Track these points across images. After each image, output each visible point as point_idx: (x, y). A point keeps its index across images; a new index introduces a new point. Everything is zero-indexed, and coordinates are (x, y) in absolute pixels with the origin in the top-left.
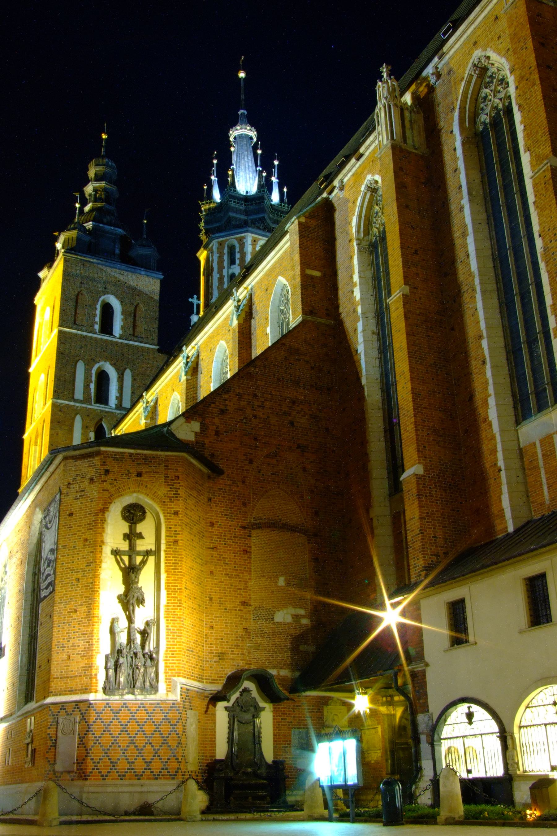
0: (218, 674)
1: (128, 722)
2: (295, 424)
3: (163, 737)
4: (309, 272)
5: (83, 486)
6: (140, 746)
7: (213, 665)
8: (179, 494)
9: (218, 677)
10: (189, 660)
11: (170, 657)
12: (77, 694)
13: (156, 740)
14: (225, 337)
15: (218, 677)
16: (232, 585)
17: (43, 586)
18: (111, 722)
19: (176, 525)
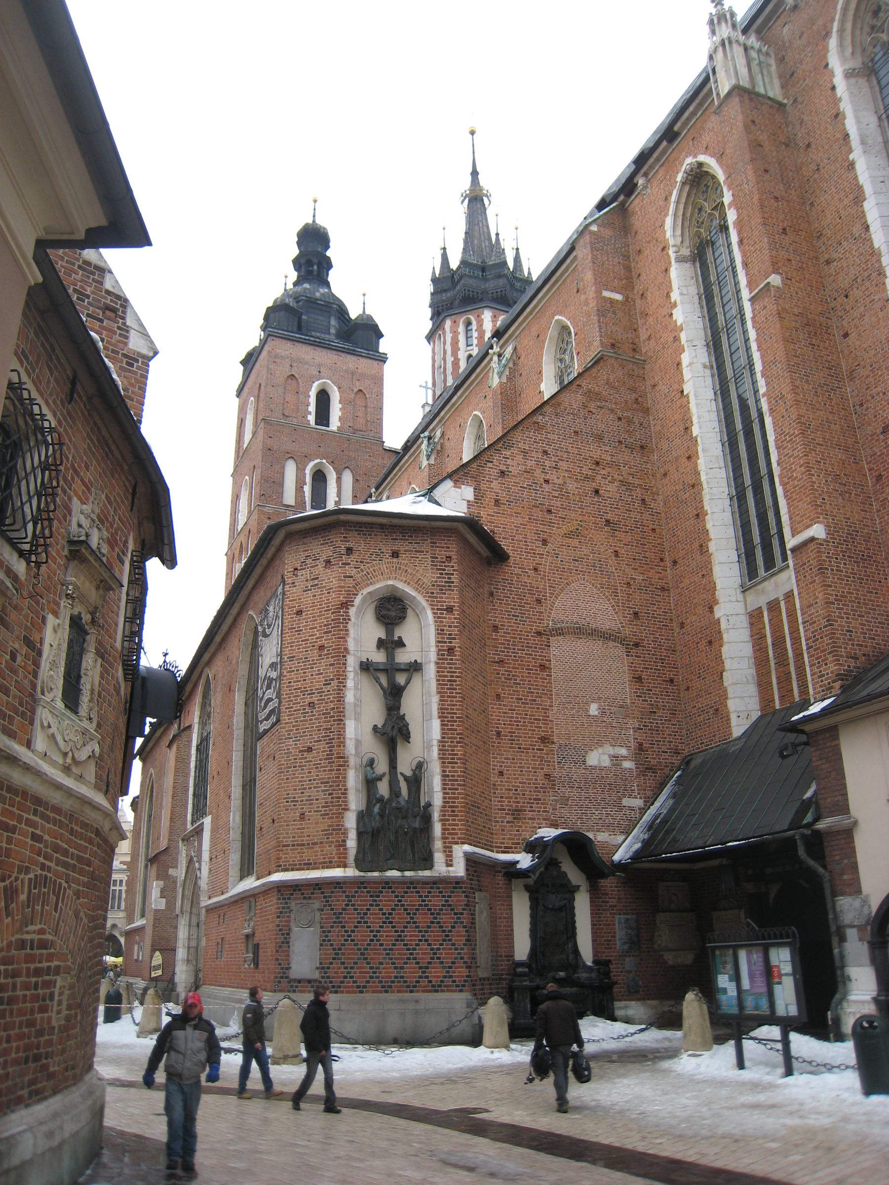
0: (513, 839)
1: (393, 910)
2: (601, 492)
3: (444, 931)
4: (606, 294)
5: (316, 571)
6: (411, 945)
7: (505, 826)
8: (453, 582)
9: (513, 844)
10: (476, 819)
11: (449, 815)
12: (318, 868)
13: (434, 936)
14: (480, 406)
15: (513, 844)
16: (526, 715)
17: (262, 715)
18: (368, 909)
19: (450, 627)
